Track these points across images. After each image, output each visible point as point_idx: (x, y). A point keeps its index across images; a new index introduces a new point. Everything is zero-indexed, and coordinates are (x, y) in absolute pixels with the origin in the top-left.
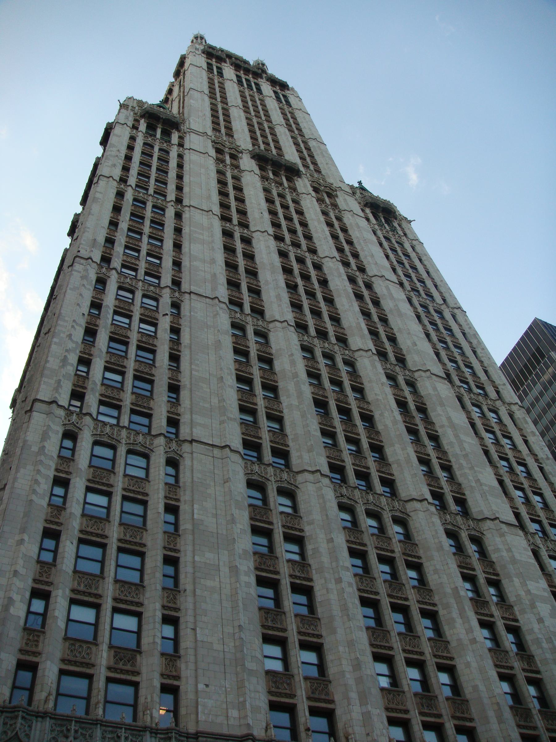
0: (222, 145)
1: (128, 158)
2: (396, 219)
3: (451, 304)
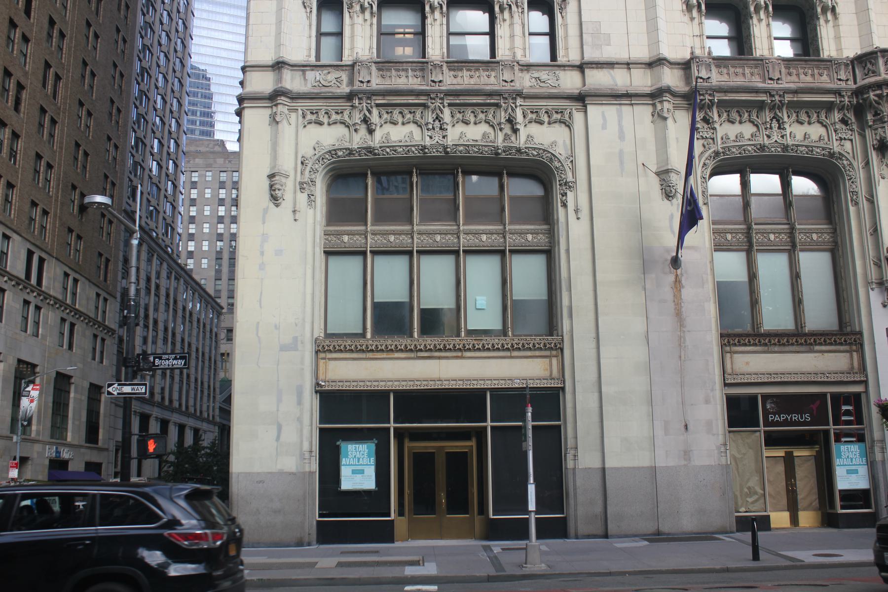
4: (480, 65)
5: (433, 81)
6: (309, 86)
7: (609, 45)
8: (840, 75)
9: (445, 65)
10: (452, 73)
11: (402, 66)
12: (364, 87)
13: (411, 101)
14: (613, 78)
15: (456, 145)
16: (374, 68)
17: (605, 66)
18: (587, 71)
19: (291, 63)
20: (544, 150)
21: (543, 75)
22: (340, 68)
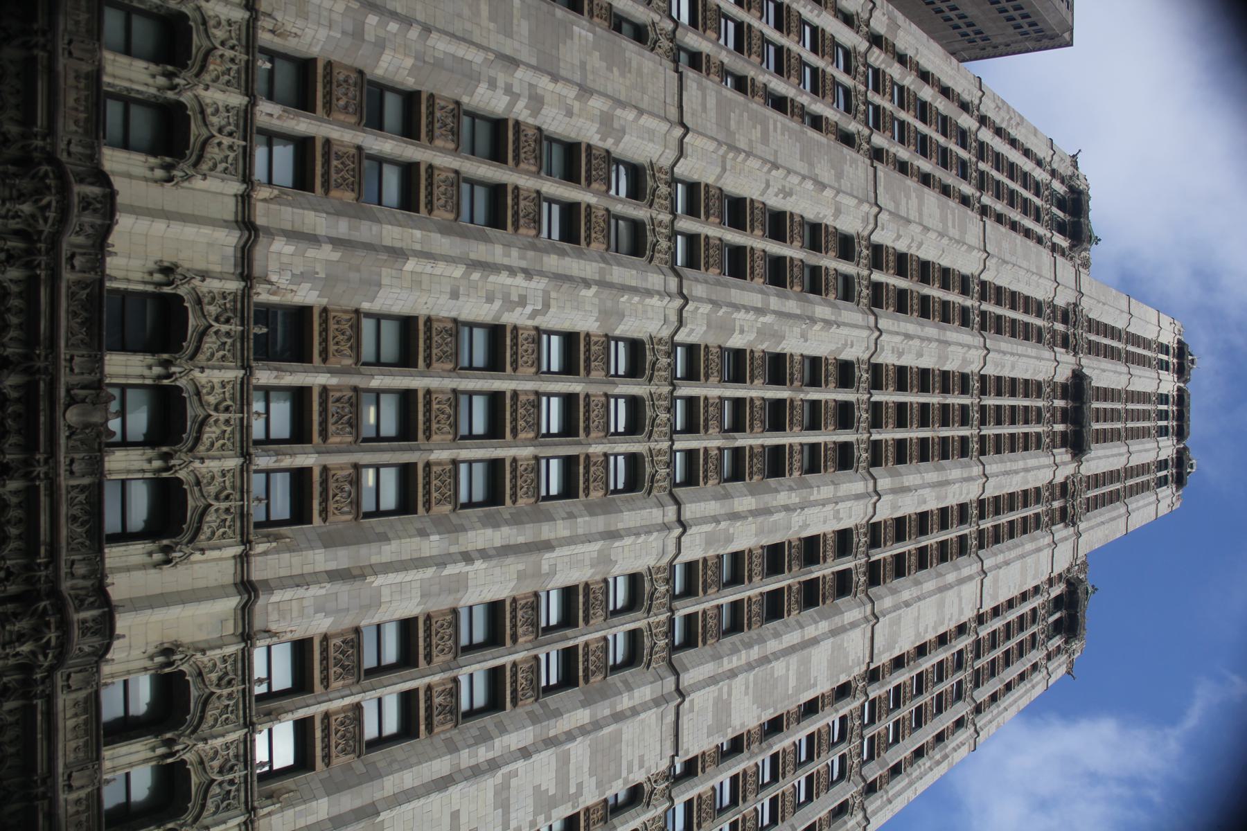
0: (1075, 322)
1: (1013, 143)
2: (1066, 642)
3: (981, 721)
8: (77, 145)
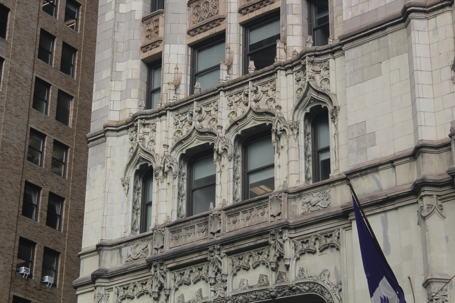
4: (253, 204)
5: (213, 234)
6: (124, 262)
7: (374, 145)
9: (223, 213)
10: (232, 219)
11: (190, 224)
12: (159, 253)
13: (195, 259)
14: (378, 183)
15: (236, 295)
16: (167, 232)
17: (369, 171)
18: (353, 182)
19: (109, 243)
20: (315, 283)
21: (314, 197)
22: (146, 238)
